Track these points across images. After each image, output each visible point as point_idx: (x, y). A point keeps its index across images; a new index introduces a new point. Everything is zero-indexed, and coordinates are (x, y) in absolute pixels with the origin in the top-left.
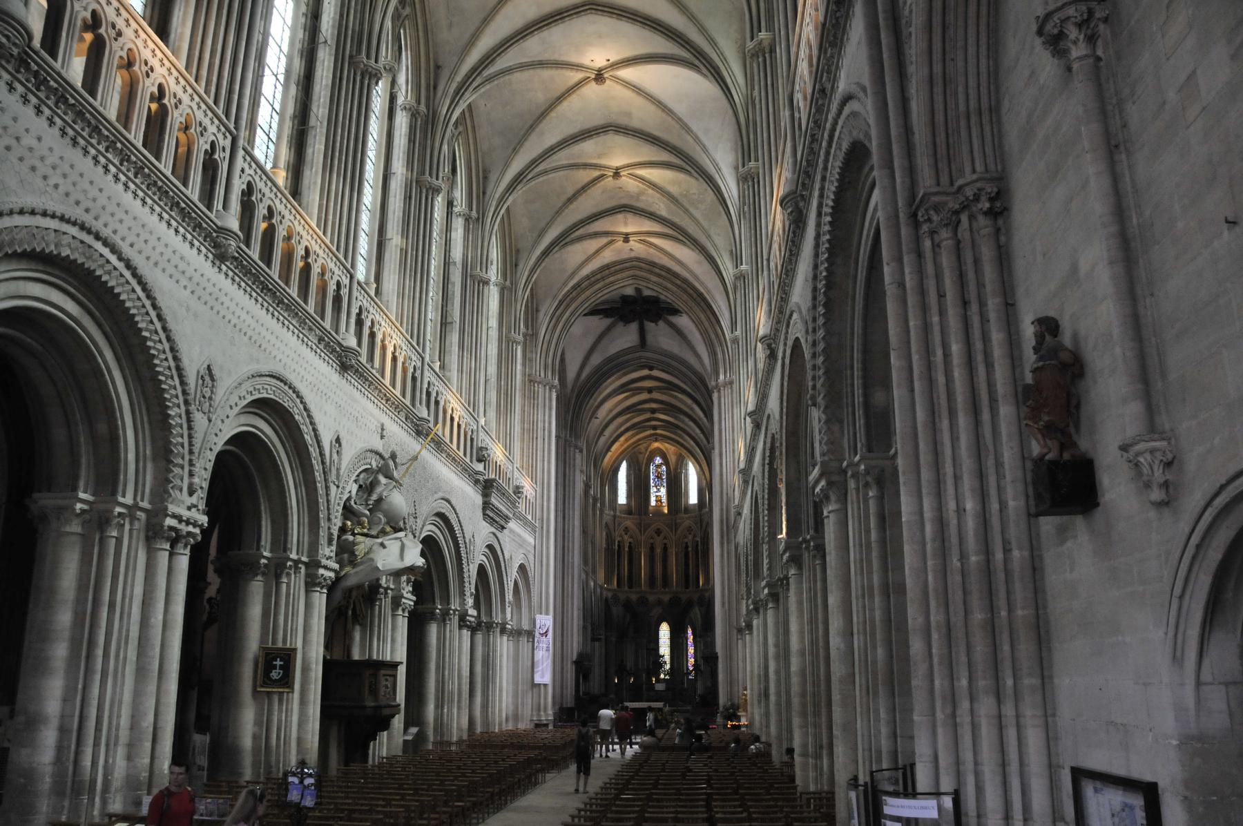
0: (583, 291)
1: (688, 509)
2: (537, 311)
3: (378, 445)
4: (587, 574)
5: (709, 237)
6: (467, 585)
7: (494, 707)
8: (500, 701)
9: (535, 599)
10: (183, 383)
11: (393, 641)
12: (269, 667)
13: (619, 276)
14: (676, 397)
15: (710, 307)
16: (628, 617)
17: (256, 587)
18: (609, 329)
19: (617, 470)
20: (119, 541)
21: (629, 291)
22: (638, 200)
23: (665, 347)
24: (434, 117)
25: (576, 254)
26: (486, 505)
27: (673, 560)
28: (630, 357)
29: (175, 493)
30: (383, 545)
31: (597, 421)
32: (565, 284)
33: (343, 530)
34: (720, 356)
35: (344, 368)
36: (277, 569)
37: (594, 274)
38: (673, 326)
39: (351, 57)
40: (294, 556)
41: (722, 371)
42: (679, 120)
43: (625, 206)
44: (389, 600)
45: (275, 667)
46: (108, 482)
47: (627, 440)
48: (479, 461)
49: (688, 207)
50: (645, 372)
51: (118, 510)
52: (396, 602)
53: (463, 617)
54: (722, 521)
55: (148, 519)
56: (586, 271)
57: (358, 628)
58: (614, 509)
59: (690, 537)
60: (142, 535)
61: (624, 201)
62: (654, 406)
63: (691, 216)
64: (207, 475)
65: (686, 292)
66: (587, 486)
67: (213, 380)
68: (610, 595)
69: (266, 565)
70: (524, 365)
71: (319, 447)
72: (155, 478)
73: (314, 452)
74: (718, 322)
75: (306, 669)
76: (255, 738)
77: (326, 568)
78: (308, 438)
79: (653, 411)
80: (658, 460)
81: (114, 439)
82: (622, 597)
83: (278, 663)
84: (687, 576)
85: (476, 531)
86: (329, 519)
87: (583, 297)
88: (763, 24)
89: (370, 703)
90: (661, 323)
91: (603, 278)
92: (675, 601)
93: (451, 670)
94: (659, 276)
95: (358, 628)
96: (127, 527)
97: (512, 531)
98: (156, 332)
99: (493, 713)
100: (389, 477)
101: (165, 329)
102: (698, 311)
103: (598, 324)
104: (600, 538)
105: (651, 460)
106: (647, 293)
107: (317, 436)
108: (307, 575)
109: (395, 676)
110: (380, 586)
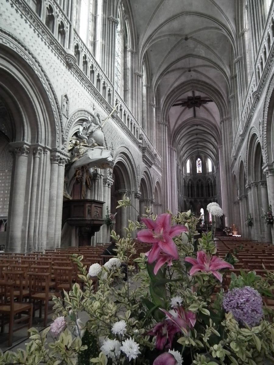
0: (175, 92)
1: (208, 173)
2: (160, 100)
4: (179, 191)
6: (137, 183)
14: (205, 136)
15: (220, 93)
17: (23, 159)
19: (186, 163)
21: (190, 94)
23: (202, 116)
26: (144, 156)
31: (180, 145)
32: (169, 90)
33: (76, 144)
34: (223, 110)
36: (34, 151)
37: (178, 86)
38: (205, 108)
40: (43, 145)
41: (224, 115)
43: (189, 55)
44: (102, 180)
47: (189, 153)
48: (140, 139)
49: (213, 49)
52: (105, 181)
56: (176, 85)
57: (89, 191)
58: (186, 174)
59: (210, 182)
61: (189, 53)
62: (198, 140)
63: (214, 53)
66: (178, 165)
70: (156, 118)
74: (223, 98)
76: (23, 232)
77: (61, 153)
79: (198, 142)
80: (199, 159)
82: (189, 200)
84: (209, 193)
85: (140, 165)
86: (62, 131)
87: (175, 94)
90: (201, 107)
91: (182, 88)
94: (201, 85)
95: (89, 191)
97: (153, 169)
102: (215, 95)
103: (179, 108)
104: (182, 184)
105: (196, 159)
108: (51, 156)
109: (101, 208)
110: (97, 174)
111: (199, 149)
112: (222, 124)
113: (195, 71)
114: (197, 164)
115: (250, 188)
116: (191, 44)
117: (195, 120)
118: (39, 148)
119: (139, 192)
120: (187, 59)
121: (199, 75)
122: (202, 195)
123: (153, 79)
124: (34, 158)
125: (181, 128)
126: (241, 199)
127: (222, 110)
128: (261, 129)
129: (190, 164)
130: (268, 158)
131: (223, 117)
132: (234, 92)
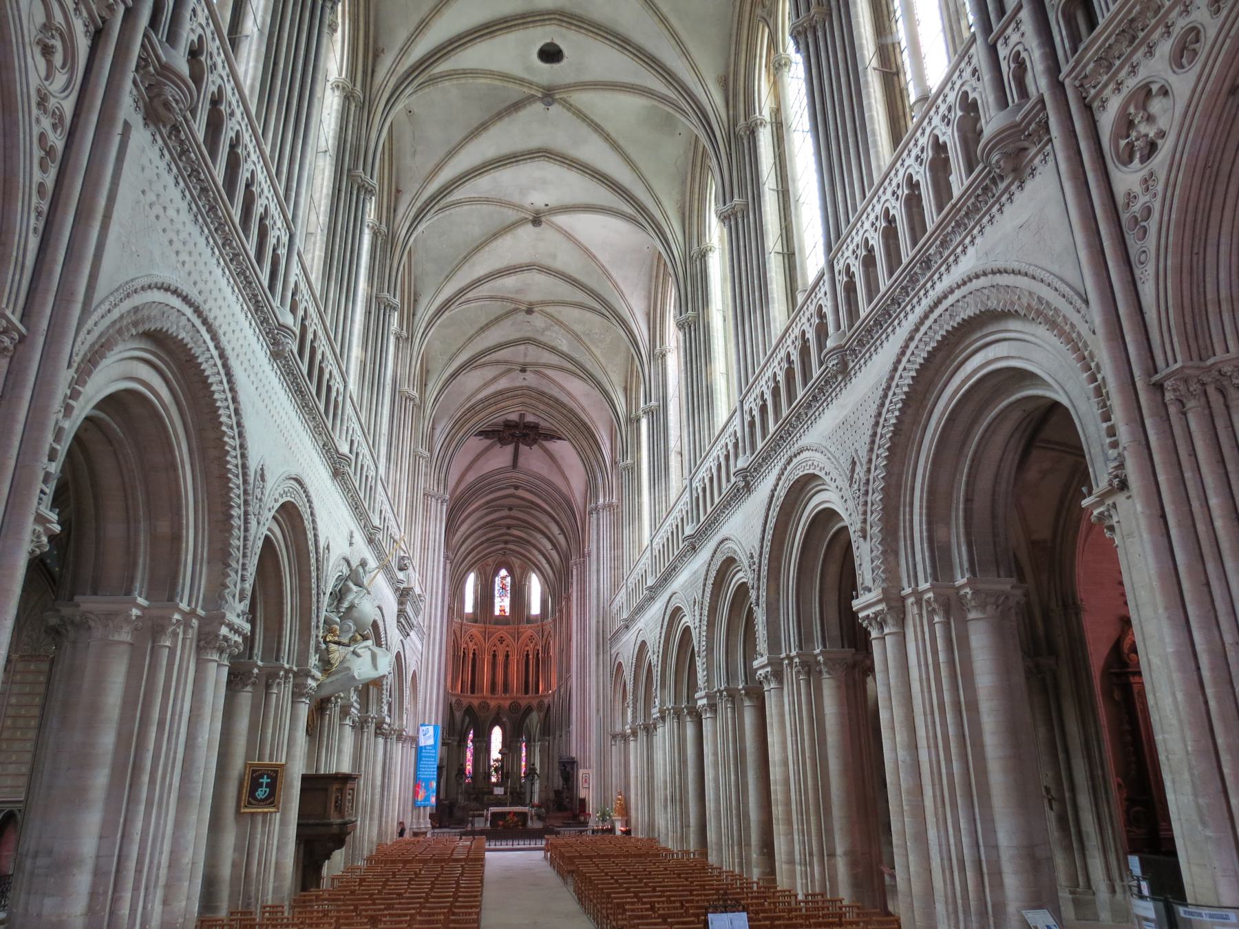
0: (477, 413)
1: (529, 620)
3: (347, 551)
5: (606, 373)
7: (387, 817)
8: (393, 810)
9: (420, 706)
10: (245, 482)
11: (339, 751)
12: (255, 785)
13: (510, 403)
14: (534, 516)
15: (593, 436)
16: (467, 719)
18: (487, 449)
19: (465, 582)
20: (172, 651)
21: (514, 417)
22: (542, 334)
24: (393, 238)
25: (473, 380)
26: (401, 613)
27: (514, 668)
28: (501, 476)
29: (230, 599)
30: (354, 653)
35: (337, 474)
37: (487, 398)
38: (546, 451)
39: (349, 170)
42: (602, 267)
43: (529, 339)
44: (338, 709)
45: (261, 785)
46: (165, 585)
47: (478, 553)
50: (512, 491)
51: (177, 616)
52: (345, 712)
53: (379, 727)
54: (598, 633)
55: (199, 627)
60: (194, 646)
61: (528, 335)
63: (592, 354)
64: (252, 582)
65: (571, 420)
67: (263, 480)
68: (454, 700)
69: (258, 676)
71: (317, 553)
72: (209, 581)
73: (313, 561)
75: (291, 786)
76: (234, 865)
77: (313, 678)
78: (311, 543)
80: (503, 572)
81: (176, 538)
82: (465, 702)
83: (265, 780)
86: (318, 627)
88: (736, 191)
89: (335, 820)
90: (535, 447)
91: (496, 403)
92: (515, 707)
93: (366, 780)
96: (181, 636)
98: (232, 428)
99: (387, 823)
100: (359, 585)
101: (239, 424)
105: (496, 573)
106: (530, 418)
107: (316, 541)
108: (295, 686)
111: (511, 546)
112: (595, 515)
113: (536, 372)
114: (497, 588)
115: (663, 718)
116: (538, 321)
117: (514, 475)
118: (282, 673)
119: (388, 720)
120: (522, 347)
121: (545, 381)
122: (506, 688)
123: (430, 386)
124: (268, 695)
125: (473, 494)
126: (634, 733)
127: (596, 479)
128: (697, 613)
129: (476, 586)
130: (707, 681)
131: (597, 498)
132: (632, 458)
